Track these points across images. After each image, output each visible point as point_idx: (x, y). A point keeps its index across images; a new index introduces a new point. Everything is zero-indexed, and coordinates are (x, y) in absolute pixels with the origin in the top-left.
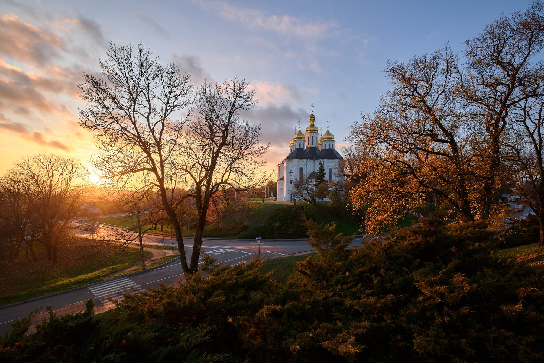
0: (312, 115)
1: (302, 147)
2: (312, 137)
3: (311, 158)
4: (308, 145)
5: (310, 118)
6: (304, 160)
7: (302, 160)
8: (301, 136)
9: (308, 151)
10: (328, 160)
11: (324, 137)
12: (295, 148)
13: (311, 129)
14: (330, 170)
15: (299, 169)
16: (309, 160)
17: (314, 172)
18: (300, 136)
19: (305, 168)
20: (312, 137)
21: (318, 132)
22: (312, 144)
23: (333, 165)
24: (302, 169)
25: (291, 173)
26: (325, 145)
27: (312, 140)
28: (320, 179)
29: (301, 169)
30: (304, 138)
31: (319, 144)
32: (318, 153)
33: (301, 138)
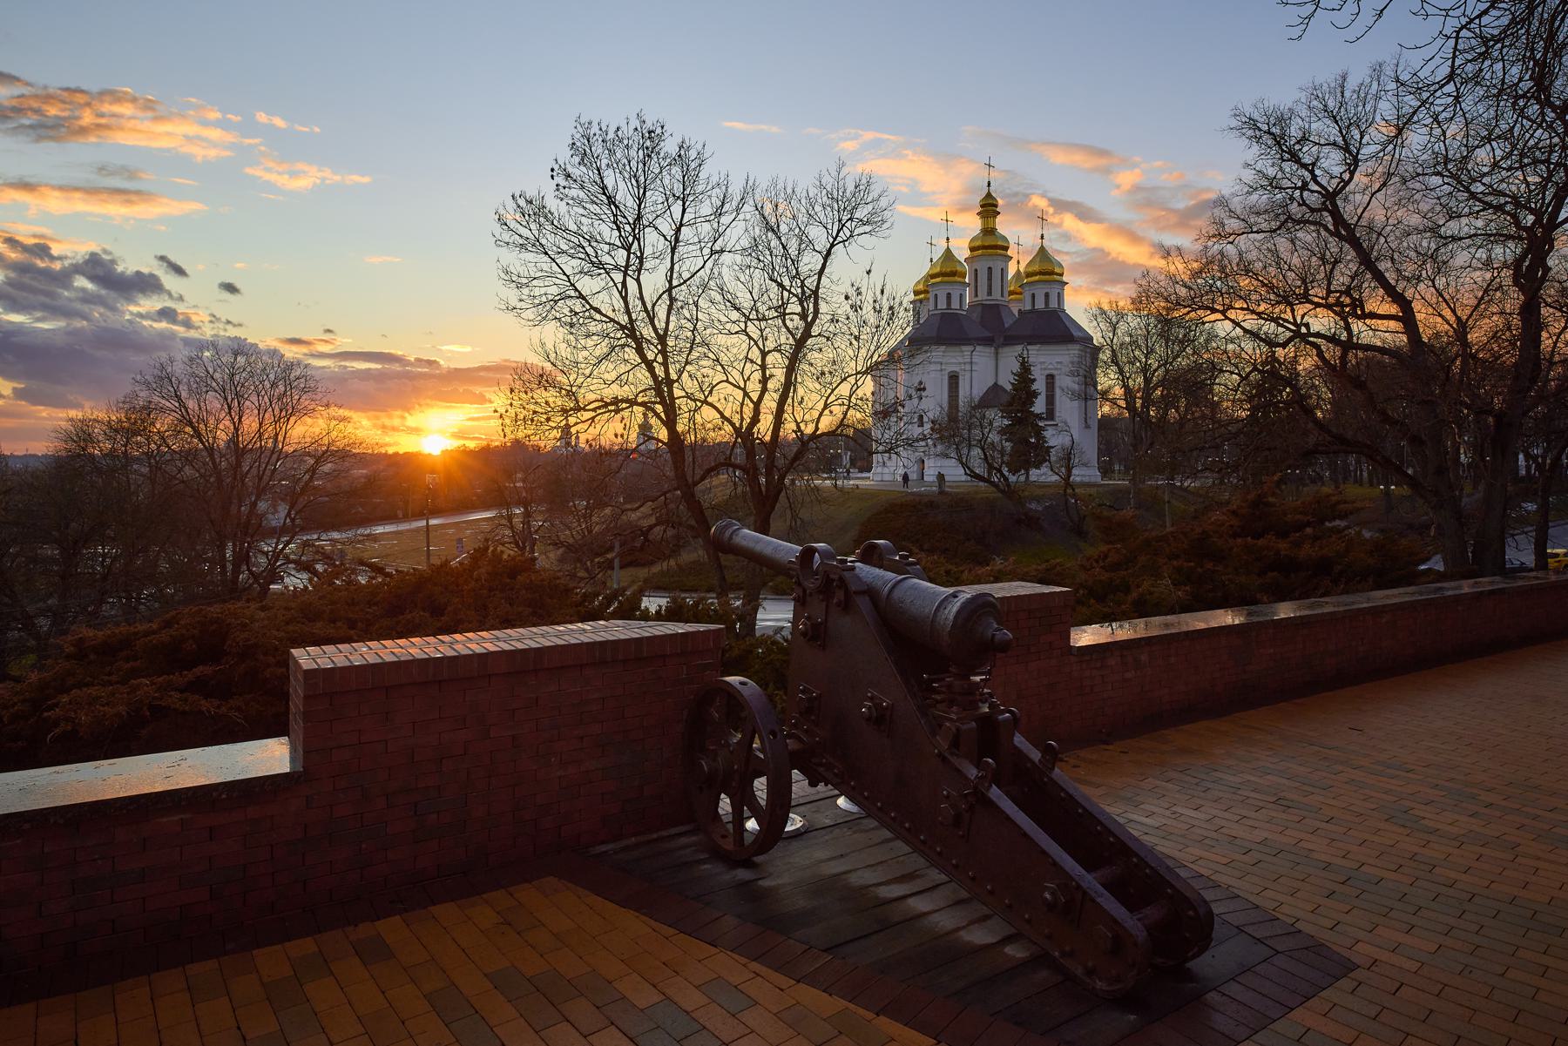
0: (989, 195)
1: (955, 305)
3: (987, 341)
4: (976, 296)
6: (964, 348)
7: (957, 349)
9: (975, 316)
10: (1044, 347)
11: (1030, 270)
14: (1050, 379)
15: (947, 377)
16: (978, 348)
17: (996, 387)
19: (968, 375)
22: (990, 293)
23: (1058, 363)
24: (958, 377)
25: (919, 390)
26: (1033, 296)
27: (990, 279)
28: (1018, 411)
29: (954, 379)
31: (1011, 293)
32: (1008, 322)
33: (954, 274)
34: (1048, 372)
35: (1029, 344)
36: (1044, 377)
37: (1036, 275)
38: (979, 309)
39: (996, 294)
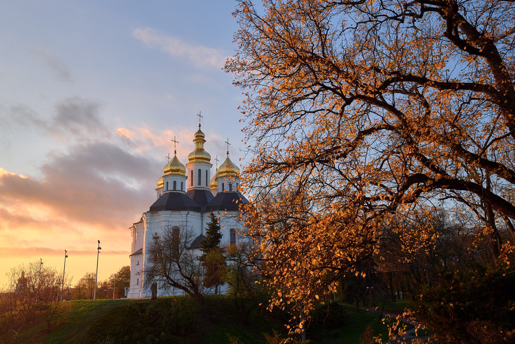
0: (200, 131)
1: (178, 188)
2: (200, 170)
3: (197, 209)
5: (197, 137)
8: (178, 168)
9: (191, 196)
11: (222, 170)
12: (165, 189)
13: (198, 156)
16: (191, 213)
18: (175, 168)
20: (200, 170)
21: (211, 162)
22: (199, 184)
26: (223, 184)
27: (200, 176)
30: (184, 172)
32: (209, 200)
34: (230, 228)
35: (220, 210)
36: (229, 230)
37: (224, 173)
38: (193, 192)
39: (203, 184)
